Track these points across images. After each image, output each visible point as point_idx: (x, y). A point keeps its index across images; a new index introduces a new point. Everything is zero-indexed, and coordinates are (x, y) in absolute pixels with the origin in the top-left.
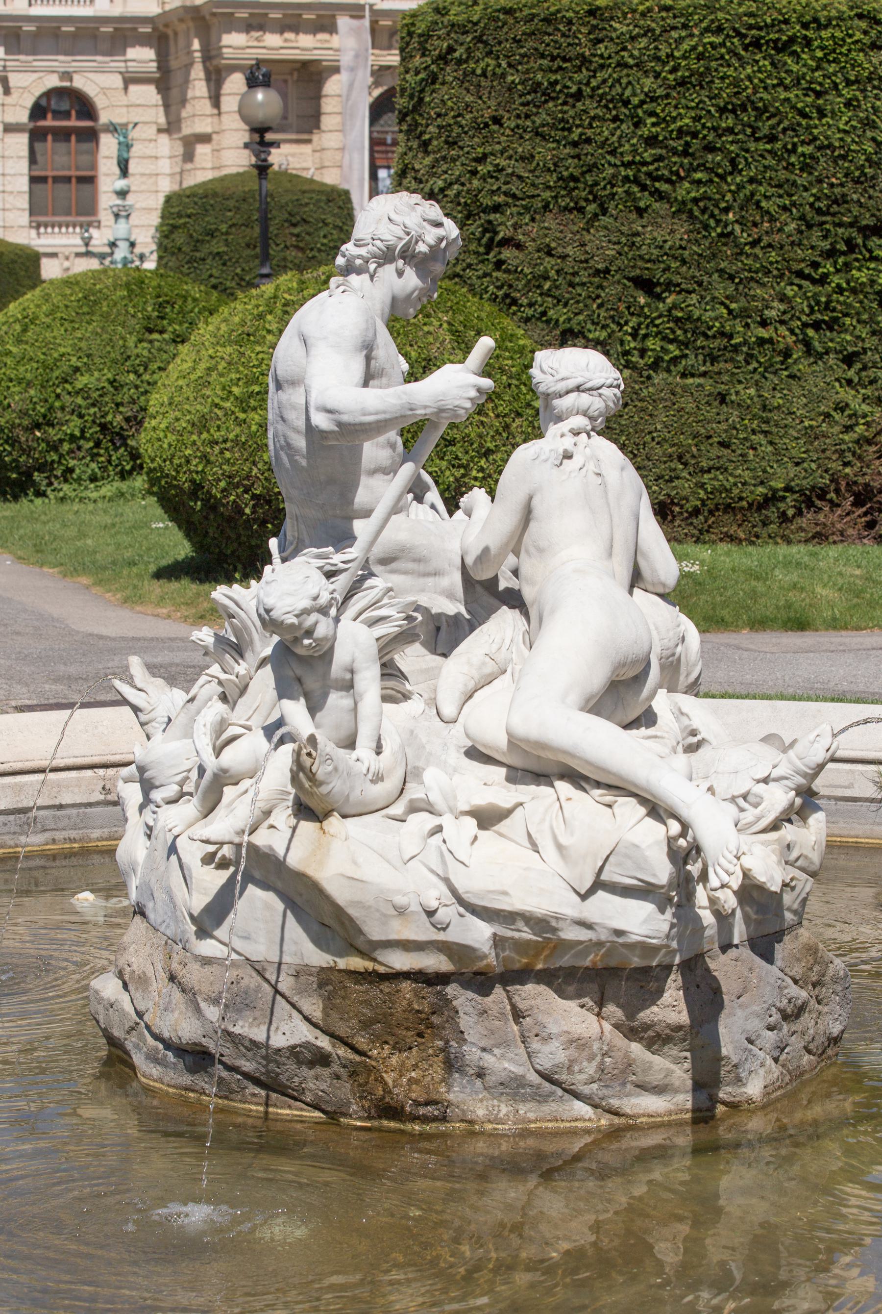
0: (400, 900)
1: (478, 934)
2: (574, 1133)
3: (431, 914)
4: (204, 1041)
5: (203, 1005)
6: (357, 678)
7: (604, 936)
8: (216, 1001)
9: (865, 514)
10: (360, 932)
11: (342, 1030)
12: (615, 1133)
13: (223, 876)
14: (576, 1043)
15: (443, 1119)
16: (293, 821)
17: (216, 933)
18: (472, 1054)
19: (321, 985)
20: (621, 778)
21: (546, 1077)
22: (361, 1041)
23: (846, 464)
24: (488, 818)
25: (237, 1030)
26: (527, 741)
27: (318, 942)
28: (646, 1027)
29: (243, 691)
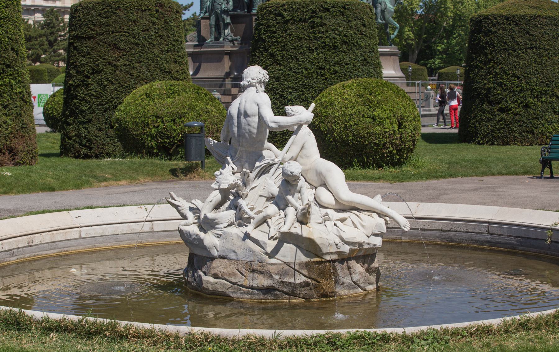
0: (331, 242)
1: (346, 249)
2: (359, 296)
3: (337, 245)
5: (273, 276)
6: (302, 189)
7: (372, 246)
8: (277, 274)
9: (11, 157)
10: (321, 251)
11: (314, 276)
12: (366, 295)
13: (276, 242)
14: (361, 274)
15: (334, 296)
18: (341, 279)
19: (306, 266)
20: (374, 208)
21: (355, 283)
22: (318, 279)
23: (7, 141)
24: (343, 220)
25: (285, 280)
26: (348, 202)
27: (306, 255)
28: (371, 268)
29: (247, 196)
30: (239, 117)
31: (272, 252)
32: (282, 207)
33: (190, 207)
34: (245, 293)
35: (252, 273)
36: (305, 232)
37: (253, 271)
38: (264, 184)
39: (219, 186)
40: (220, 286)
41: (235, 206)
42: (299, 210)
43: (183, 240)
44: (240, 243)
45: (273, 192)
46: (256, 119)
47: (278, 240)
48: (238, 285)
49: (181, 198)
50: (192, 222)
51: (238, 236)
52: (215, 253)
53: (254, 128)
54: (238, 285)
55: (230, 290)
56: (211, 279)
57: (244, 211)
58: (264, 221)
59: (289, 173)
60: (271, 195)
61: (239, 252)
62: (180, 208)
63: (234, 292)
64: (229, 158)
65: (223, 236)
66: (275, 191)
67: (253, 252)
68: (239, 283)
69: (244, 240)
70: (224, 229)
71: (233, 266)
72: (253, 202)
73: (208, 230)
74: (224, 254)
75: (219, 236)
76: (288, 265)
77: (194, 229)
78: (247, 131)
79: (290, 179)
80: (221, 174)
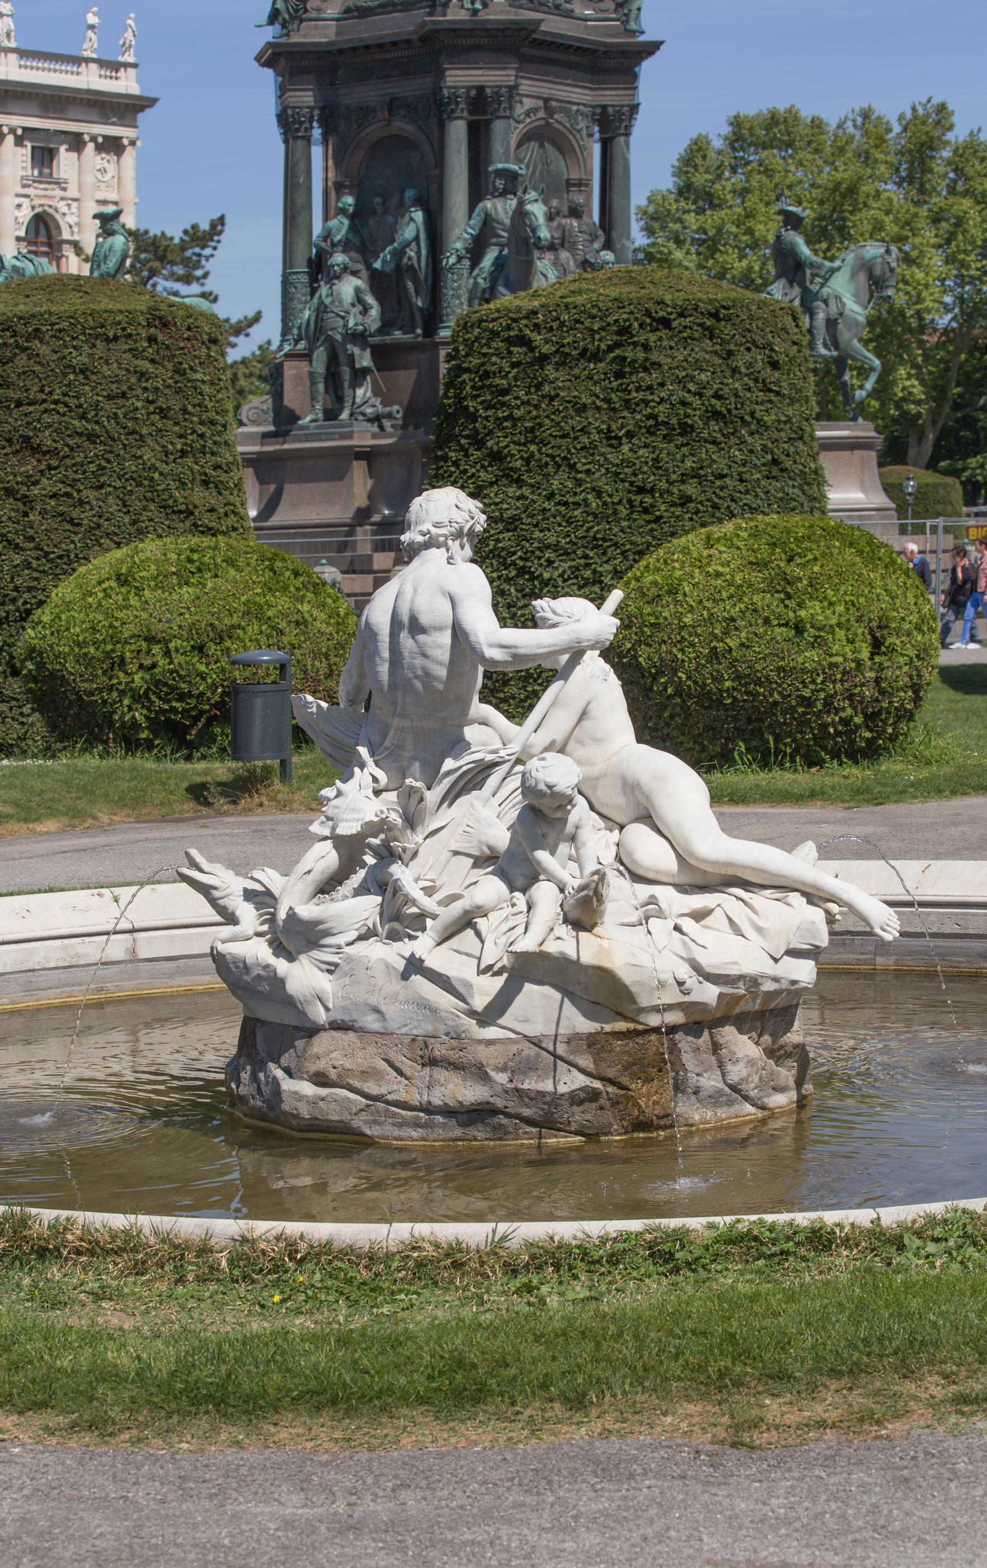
4: (491, 1100)
5: (492, 1074)
8: (503, 1069)
13: (500, 981)
16: (574, 933)
17: (500, 1021)
30: (394, 635)
31: (486, 1008)
32: (520, 882)
33: (245, 890)
34: (408, 1125)
35: (428, 1069)
36: (588, 949)
37: (432, 1062)
38: (466, 821)
40: (333, 1106)
41: (378, 883)
42: (569, 889)
43: (225, 981)
44: (395, 986)
45: (492, 842)
46: (445, 638)
47: (505, 975)
48: (388, 1103)
49: (219, 866)
50: (251, 932)
51: (387, 966)
52: (320, 1016)
53: (441, 664)
54: (388, 1103)
55: (363, 1117)
56: (307, 1088)
57: (406, 896)
58: (467, 921)
60: (487, 851)
61: (391, 1010)
62: (216, 894)
63: (375, 1122)
65: (345, 967)
66: (501, 837)
67: (431, 1010)
68: (389, 1097)
69: (405, 976)
70: (347, 949)
71: (372, 1050)
72: (433, 869)
73: (300, 953)
74: (347, 1018)
75: (331, 969)
76: (536, 1042)
77: (258, 951)
78: (419, 672)
79: (544, 805)
80: (339, 794)
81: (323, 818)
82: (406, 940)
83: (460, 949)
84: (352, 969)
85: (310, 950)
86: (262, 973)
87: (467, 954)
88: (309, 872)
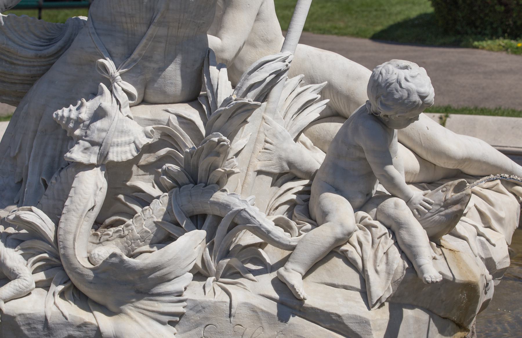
39: (103, 156)
47: (387, 304)
51: (254, 310)
59: (416, 98)
64: (109, 63)
80: (100, 114)
81: (87, 144)
82: (251, 276)
83: (336, 282)
84: (207, 318)
85: (138, 299)
86: (76, 333)
87: (346, 287)
88: (93, 208)
